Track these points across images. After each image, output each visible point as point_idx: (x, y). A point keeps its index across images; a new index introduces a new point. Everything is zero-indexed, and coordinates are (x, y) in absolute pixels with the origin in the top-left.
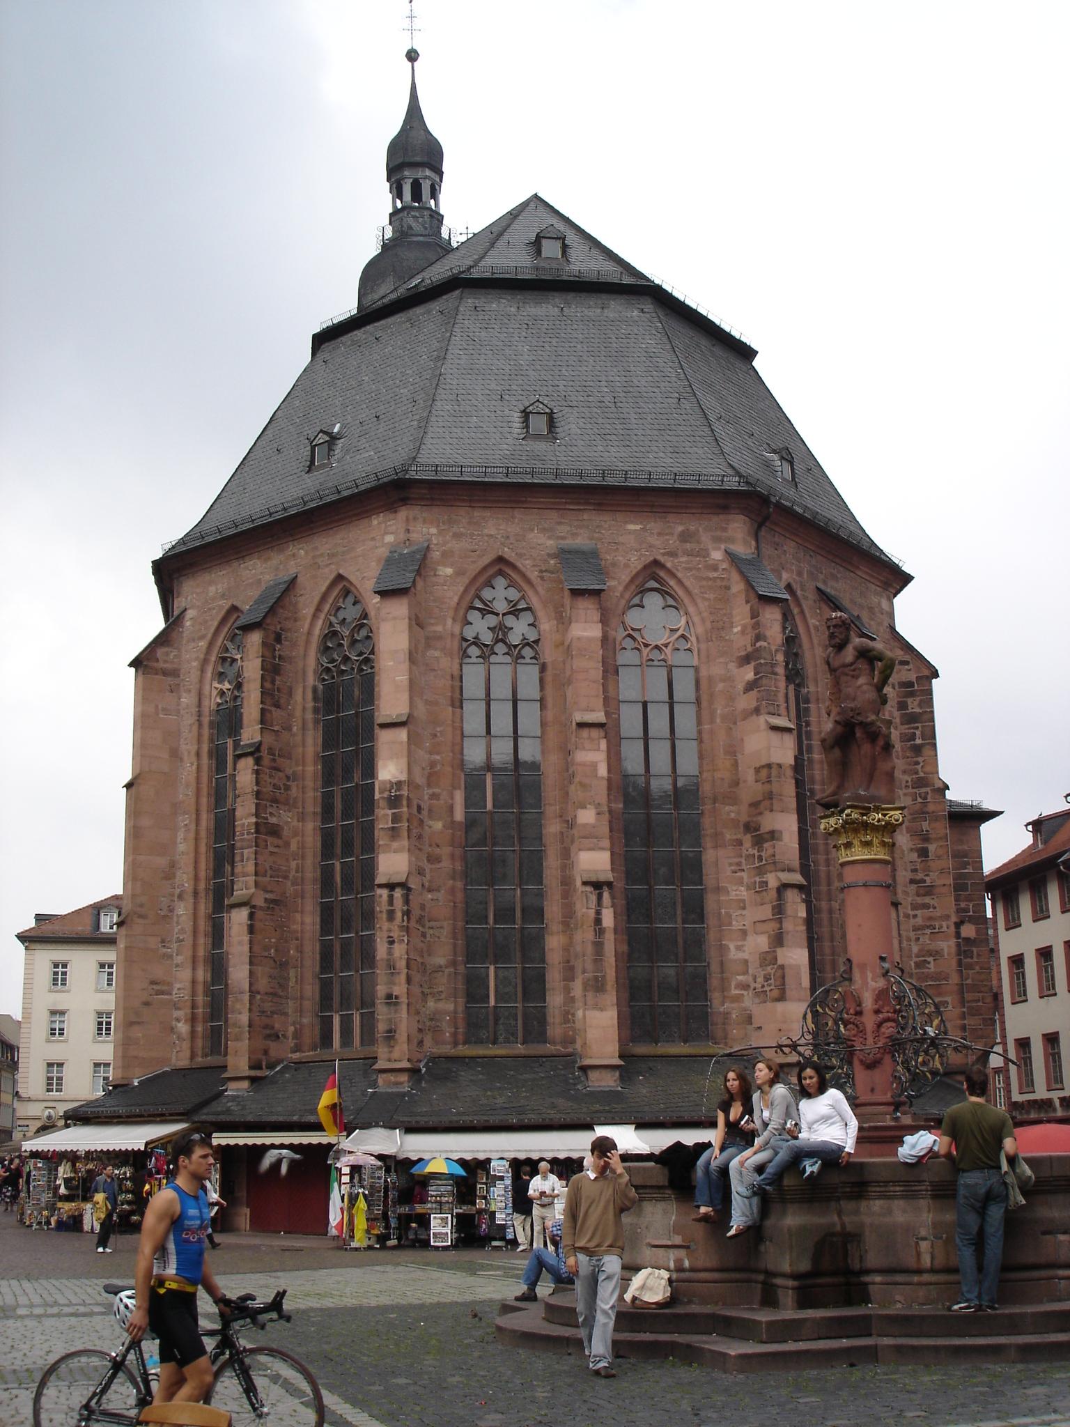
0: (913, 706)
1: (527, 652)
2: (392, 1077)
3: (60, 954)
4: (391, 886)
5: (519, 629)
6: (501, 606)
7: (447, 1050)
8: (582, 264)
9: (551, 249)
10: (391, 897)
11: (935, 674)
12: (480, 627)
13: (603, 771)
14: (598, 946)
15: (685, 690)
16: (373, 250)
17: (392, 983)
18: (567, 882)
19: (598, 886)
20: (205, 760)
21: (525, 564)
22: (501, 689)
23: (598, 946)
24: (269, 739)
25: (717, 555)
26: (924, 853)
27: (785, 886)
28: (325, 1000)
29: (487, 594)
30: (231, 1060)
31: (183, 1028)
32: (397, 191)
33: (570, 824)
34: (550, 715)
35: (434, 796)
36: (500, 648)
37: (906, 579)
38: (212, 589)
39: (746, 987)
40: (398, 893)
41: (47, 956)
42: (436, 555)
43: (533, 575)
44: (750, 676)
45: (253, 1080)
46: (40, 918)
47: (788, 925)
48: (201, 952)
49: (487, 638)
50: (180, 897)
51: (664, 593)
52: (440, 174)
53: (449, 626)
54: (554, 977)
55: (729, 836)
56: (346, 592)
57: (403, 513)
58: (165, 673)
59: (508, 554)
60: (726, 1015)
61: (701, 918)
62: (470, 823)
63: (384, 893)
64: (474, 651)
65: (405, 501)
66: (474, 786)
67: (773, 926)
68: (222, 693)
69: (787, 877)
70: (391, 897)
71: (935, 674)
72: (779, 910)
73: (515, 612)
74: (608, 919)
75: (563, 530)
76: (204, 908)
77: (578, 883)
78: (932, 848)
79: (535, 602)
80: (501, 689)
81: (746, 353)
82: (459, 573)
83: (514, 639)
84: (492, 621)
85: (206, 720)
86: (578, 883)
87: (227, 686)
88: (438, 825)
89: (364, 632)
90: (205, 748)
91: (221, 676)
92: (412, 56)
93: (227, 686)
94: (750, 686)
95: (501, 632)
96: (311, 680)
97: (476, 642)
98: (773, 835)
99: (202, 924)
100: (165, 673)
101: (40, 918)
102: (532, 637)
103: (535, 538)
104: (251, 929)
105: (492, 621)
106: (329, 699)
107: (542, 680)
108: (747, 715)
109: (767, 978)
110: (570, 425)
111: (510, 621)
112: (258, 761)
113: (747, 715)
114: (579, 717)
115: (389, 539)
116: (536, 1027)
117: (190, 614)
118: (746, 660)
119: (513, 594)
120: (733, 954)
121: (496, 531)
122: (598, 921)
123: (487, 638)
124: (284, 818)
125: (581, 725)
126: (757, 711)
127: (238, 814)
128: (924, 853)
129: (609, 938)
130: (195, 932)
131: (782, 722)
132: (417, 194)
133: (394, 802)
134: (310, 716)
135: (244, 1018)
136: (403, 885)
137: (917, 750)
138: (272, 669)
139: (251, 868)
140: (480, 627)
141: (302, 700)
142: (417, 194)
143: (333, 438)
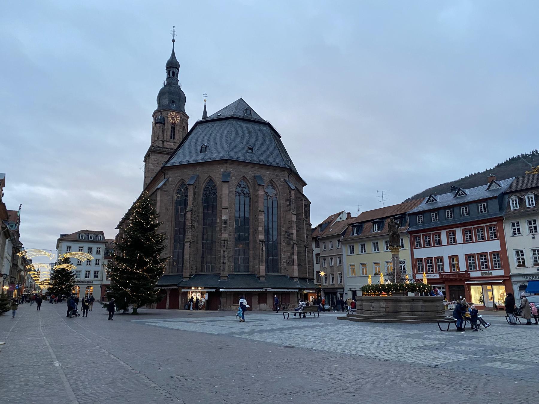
0: (306, 210)
2: (224, 278)
3: (69, 244)
4: (225, 240)
5: (246, 191)
6: (242, 186)
7: (231, 273)
8: (254, 117)
9: (248, 112)
10: (224, 243)
12: (239, 190)
14: (262, 254)
15: (275, 205)
16: (162, 86)
17: (224, 260)
18: (255, 241)
19: (262, 242)
20: (173, 210)
21: (248, 178)
23: (262, 254)
24: (194, 208)
25: (282, 180)
27: (294, 244)
28: (202, 263)
29: (240, 183)
30: (184, 274)
32: (169, 73)
33: (257, 229)
34: (251, 208)
36: (242, 194)
38: (177, 175)
40: (226, 242)
41: (64, 245)
42: (232, 174)
43: (250, 180)
45: (189, 278)
46: (62, 235)
48: (172, 251)
49: (240, 192)
51: (272, 186)
52: (179, 70)
53: (234, 189)
54: (251, 259)
56: (211, 180)
57: (225, 165)
58: (165, 191)
59: (245, 176)
60: (281, 267)
61: (277, 248)
62: (236, 228)
63: (223, 242)
64: (237, 194)
65: (226, 163)
66: (237, 221)
67: (292, 251)
68: (178, 197)
69: (294, 242)
70: (224, 243)
72: (293, 248)
73: (245, 188)
74: (264, 249)
75: (255, 172)
76: (173, 241)
77: (258, 241)
79: (249, 185)
80: (242, 203)
82: (236, 179)
83: (245, 192)
84: (241, 189)
85: (174, 202)
86: (258, 241)
89: (214, 188)
90: (174, 208)
91: (177, 193)
92: (173, 41)
93: (179, 195)
94: (288, 206)
96: (201, 196)
97: (238, 192)
98: (292, 234)
99: (172, 245)
100: (165, 191)
101: (62, 235)
102: (248, 192)
103: (250, 173)
104: (190, 247)
105: (241, 189)
106: (205, 201)
107: (250, 201)
108: (287, 211)
109: (290, 261)
110: (256, 151)
111: (244, 189)
113: (287, 211)
114: (260, 209)
116: (247, 269)
117: (171, 179)
118: (288, 200)
119: (245, 183)
120: (283, 256)
121: (244, 170)
122: (262, 249)
124: (195, 224)
125: (260, 211)
126: (290, 210)
127: (187, 223)
129: (264, 252)
130: (170, 246)
131: (294, 213)
132: (173, 75)
133: (225, 224)
134: (201, 204)
135: (188, 265)
136: (227, 240)
137: (307, 218)
138: (194, 194)
139: (190, 234)
140: (239, 190)
141: (200, 200)
142: (173, 75)
143: (206, 147)
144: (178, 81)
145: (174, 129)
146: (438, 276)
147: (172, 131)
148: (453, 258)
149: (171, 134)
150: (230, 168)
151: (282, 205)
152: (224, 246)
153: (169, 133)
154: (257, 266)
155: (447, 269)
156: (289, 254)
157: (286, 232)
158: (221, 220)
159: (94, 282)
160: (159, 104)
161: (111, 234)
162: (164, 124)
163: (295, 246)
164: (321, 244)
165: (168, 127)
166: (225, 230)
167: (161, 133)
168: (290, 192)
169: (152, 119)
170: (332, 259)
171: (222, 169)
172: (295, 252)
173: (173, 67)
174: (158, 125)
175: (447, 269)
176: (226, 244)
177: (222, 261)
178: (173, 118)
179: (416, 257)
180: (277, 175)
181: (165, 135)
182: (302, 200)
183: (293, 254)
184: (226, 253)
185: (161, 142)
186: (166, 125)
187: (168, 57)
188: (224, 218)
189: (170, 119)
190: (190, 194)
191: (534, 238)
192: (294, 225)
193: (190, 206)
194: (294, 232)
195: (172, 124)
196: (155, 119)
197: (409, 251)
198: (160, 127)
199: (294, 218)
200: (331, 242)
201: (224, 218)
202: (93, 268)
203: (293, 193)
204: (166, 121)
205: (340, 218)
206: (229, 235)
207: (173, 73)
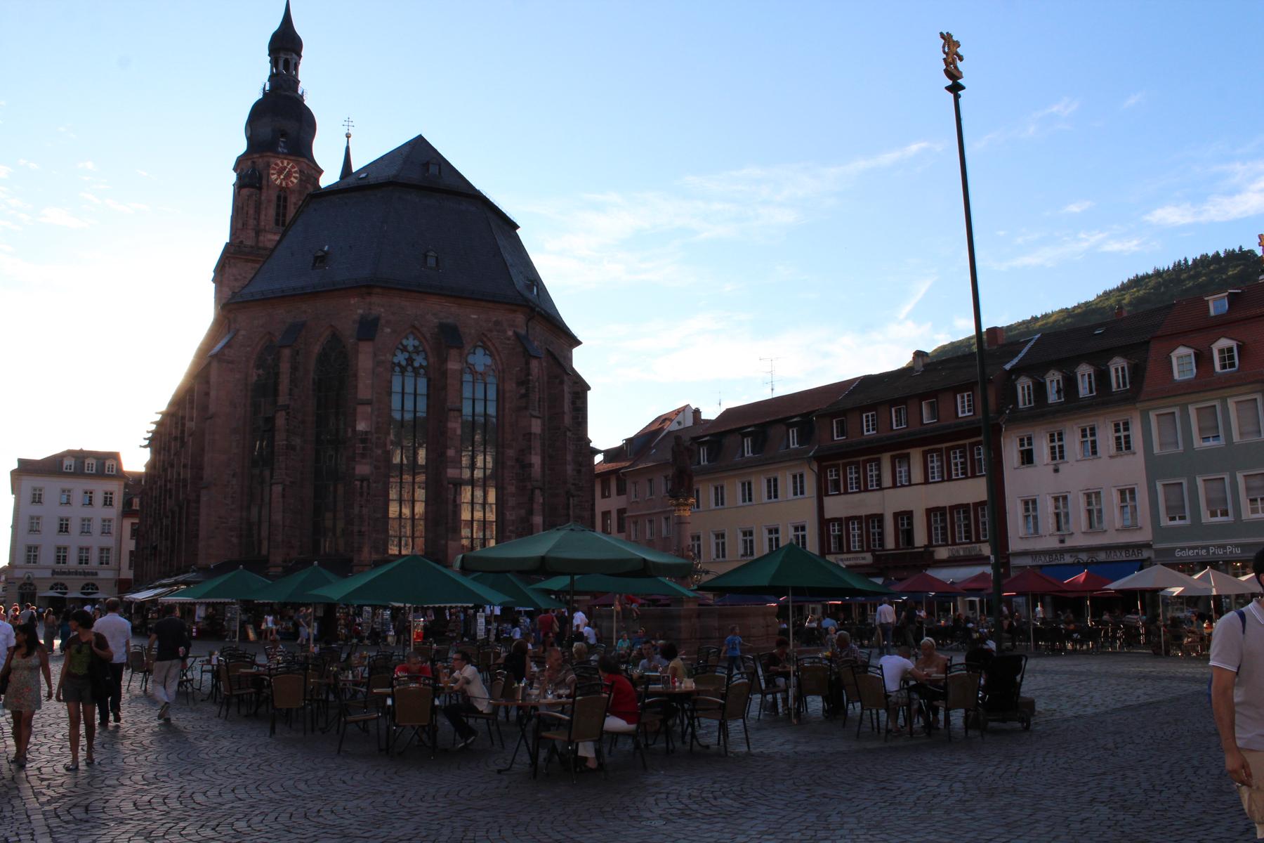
1: (422, 371)
6: (410, 349)
10: (361, 487)
11: (589, 388)
13: (459, 432)
22: (409, 389)
25: (510, 333)
26: (579, 471)
29: (405, 342)
31: (235, 540)
32: (274, 63)
35: (378, 438)
37: (578, 343)
39: (511, 532)
40: (365, 484)
43: (428, 335)
44: (523, 391)
47: (535, 506)
49: (404, 363)
50: (234, 476)
52: (300, 57)
55: (509, 463)
63: (358, 483)
64: (397, 369)
65: (370, 294)
70: (361, 487)
71: (589, 388)
72: (531, 499)
78: (583, 469)
81: (515, 226)
83: (416, 364)
84: (406, 355)
87: (261, 372)
88: (379, 452)
91: (258, 367)
94: (523, 396)
95: (410, 361)
97: (399, 365)
98: (530, 465)
104: (283, 496)
111: (414, 356)
112: (288, 414)
115: (360, 311)
117: (242, 332)
119: (416, 343)
123: (404, 363)
124: (297, 441)
126: (526, 408)
128: (579, 471)
131: (536, 413)
133: (364, 441)
138: (294, 368)
144: (297, 82)
145: (285, 199)
146: (868, 558)
147: (278, 206)
148: (904, 518)
149: (278, 214)
150: (379, 306)
151: (507, 395)
152: (361, 494)
153: (272, 212)
154: (443, 542)
155: (890, 543)
156: (523, 512)
157: (517, 460)
158: (354, 430)
159: (102, 575)
160: (249, 139)
161: (136, 460)
162: (260, 189)
163: (537, 492)
164: (630, 487)
165: (269, 196)
166: (363, 456)
167: (251, 212)
168: (527, 363)
169: (233, 177)
170: (651, 521)
171: (357, 308)
172: (537, 507)
173: (285, 46)
174: (245, 191)
175: (890, 543)
176: (365, 489)
177: (356, 529)
178: (282, 173)
179: (828, 515)
180: (497, 323)
181: (263, 217)
182: (562, 383)
183: (530, 512)
184: (365, 511)
185: (252, 234)
186: (264, 190)
187: (275, 24)
188: (361, 426)
189: (274, 177)
190: (285, 367)
191: (1056, 471)
192: (537, 444)
193: (283, 399)
194: (536, 460)
195: (280, 188)
196: (240, 178)
197: (814, 502)
198: (250, 196)
199: (536, 427)
200: (650, 481)
201: (361, 426)
202: (96, 541)
203: (534, 364)
204: (264, 182)
205: (679, 423)
206: (376, 468)
207: (287, 64)
